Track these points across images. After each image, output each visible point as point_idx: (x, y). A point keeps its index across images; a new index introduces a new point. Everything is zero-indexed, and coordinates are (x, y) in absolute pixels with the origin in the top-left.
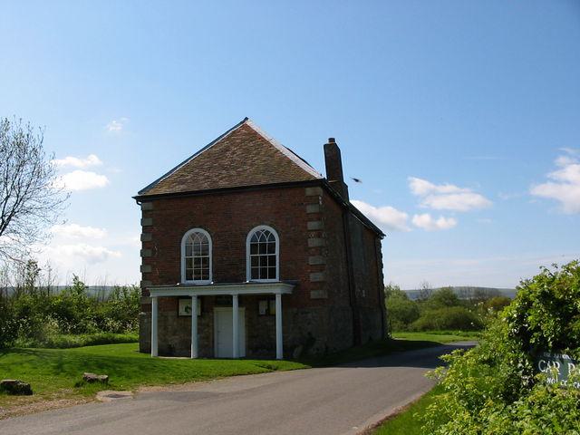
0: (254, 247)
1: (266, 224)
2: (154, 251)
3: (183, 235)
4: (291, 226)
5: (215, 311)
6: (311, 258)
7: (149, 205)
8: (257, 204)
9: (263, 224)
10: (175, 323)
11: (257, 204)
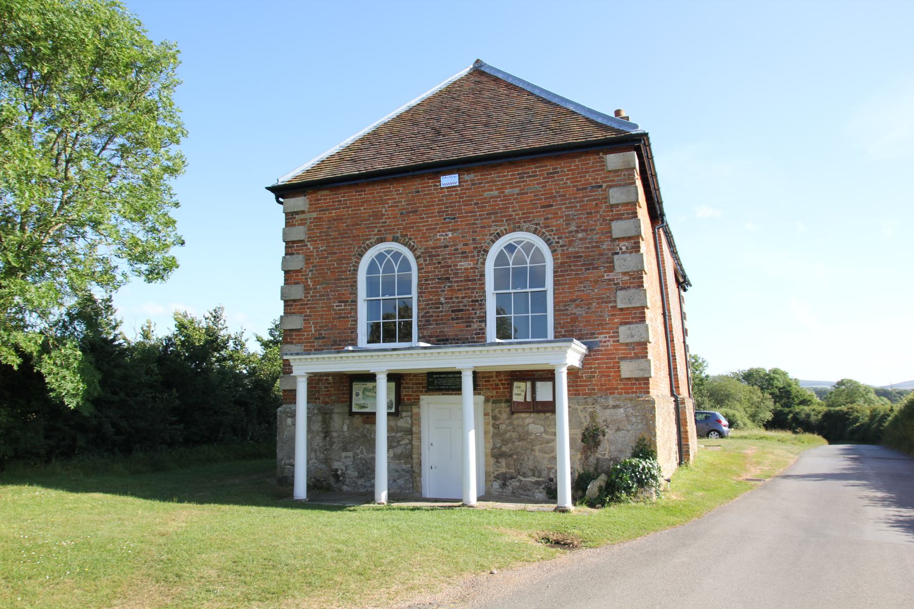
0: (501, 279)
1: (528, 230)
2: (307, 289)
3: (361, 255)
4: (577, 232)
5: (422, 403)
6: (620, 293)
7: (299, 203)
8: (507, 191)
9: (520, 229)
10: (345, 428)
11: (507, 191)
